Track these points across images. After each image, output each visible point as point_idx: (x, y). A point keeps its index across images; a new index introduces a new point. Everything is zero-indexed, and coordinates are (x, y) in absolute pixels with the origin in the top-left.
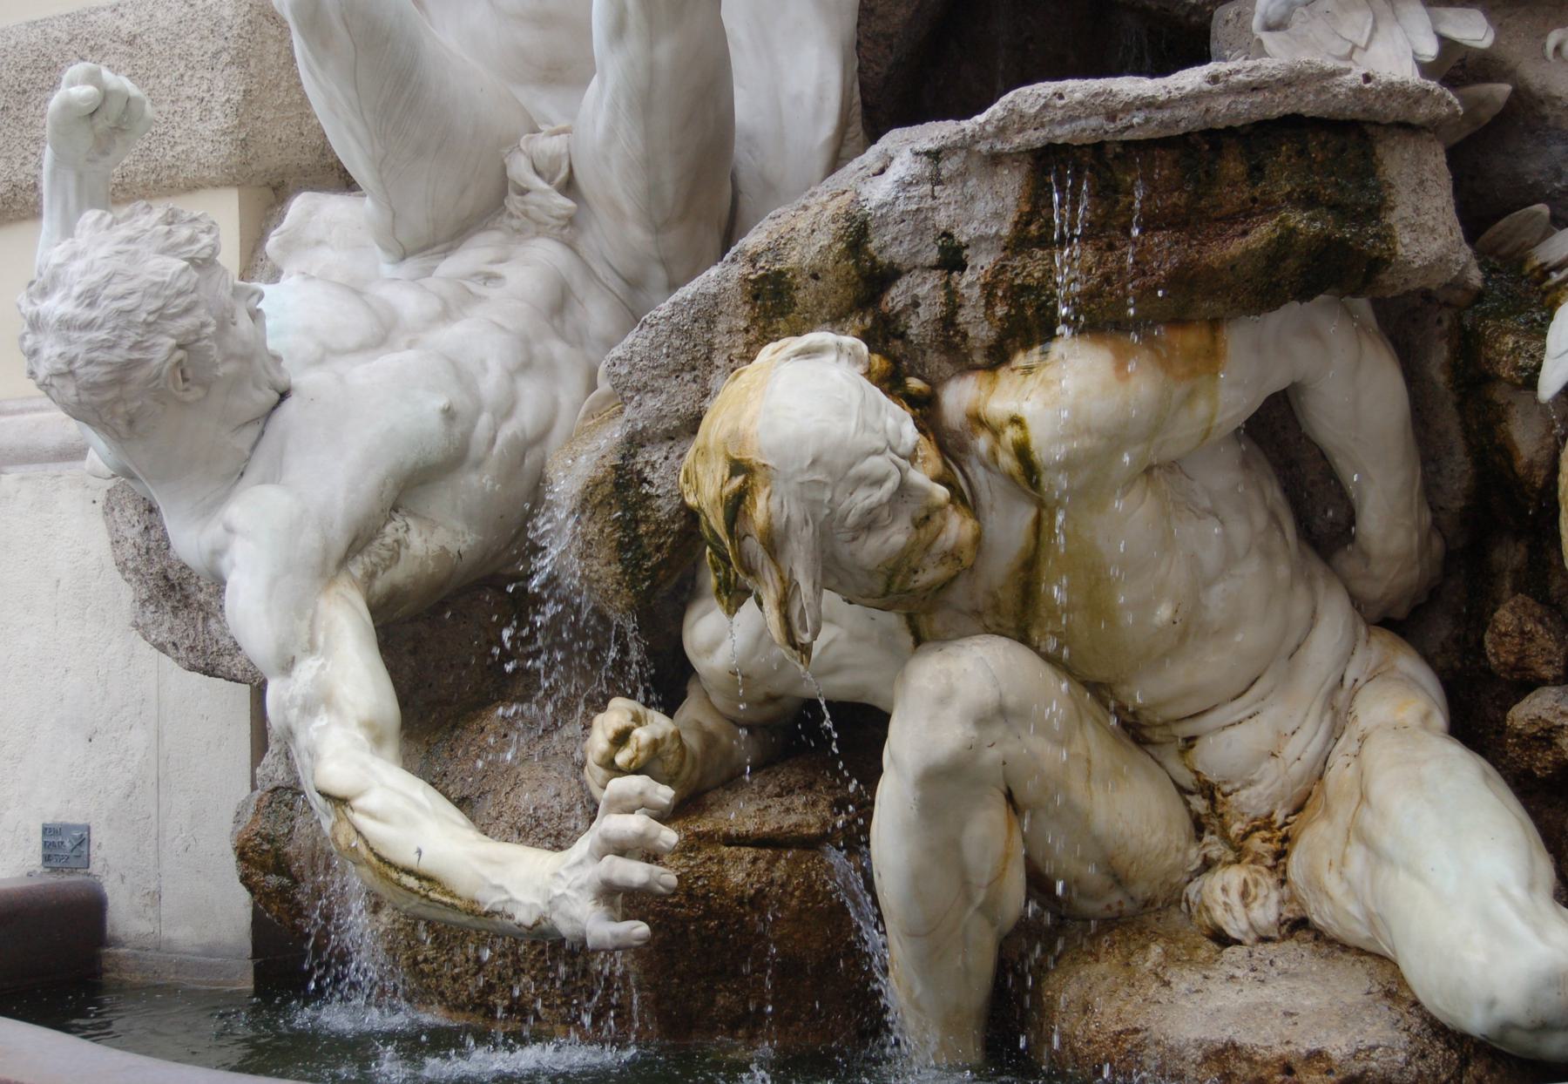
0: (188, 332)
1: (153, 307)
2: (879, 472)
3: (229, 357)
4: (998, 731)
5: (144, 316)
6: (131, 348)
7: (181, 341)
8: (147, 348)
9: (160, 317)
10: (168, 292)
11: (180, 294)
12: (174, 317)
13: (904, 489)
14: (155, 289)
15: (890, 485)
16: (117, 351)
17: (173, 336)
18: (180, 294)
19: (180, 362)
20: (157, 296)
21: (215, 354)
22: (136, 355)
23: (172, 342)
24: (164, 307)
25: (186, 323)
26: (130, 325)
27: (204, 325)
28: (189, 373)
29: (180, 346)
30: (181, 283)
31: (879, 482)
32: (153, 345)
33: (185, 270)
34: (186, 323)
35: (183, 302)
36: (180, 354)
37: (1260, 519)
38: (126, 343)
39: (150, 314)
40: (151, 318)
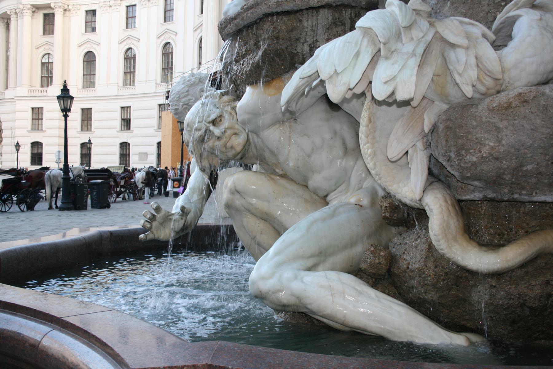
4: (238, 196)
6: (175, 105)
12: (182, 98)
15: (203, 130)
18: (183, 93)
22: (176, 107)
23: (181, 104)
25: (184, 100)
26: (174, 101)
27: (189, 100)
29: (186, 104)
30: (182, 91)
31: (199, 130)
35: (183, 95)
36: (185, 106)
37: (328, 136)
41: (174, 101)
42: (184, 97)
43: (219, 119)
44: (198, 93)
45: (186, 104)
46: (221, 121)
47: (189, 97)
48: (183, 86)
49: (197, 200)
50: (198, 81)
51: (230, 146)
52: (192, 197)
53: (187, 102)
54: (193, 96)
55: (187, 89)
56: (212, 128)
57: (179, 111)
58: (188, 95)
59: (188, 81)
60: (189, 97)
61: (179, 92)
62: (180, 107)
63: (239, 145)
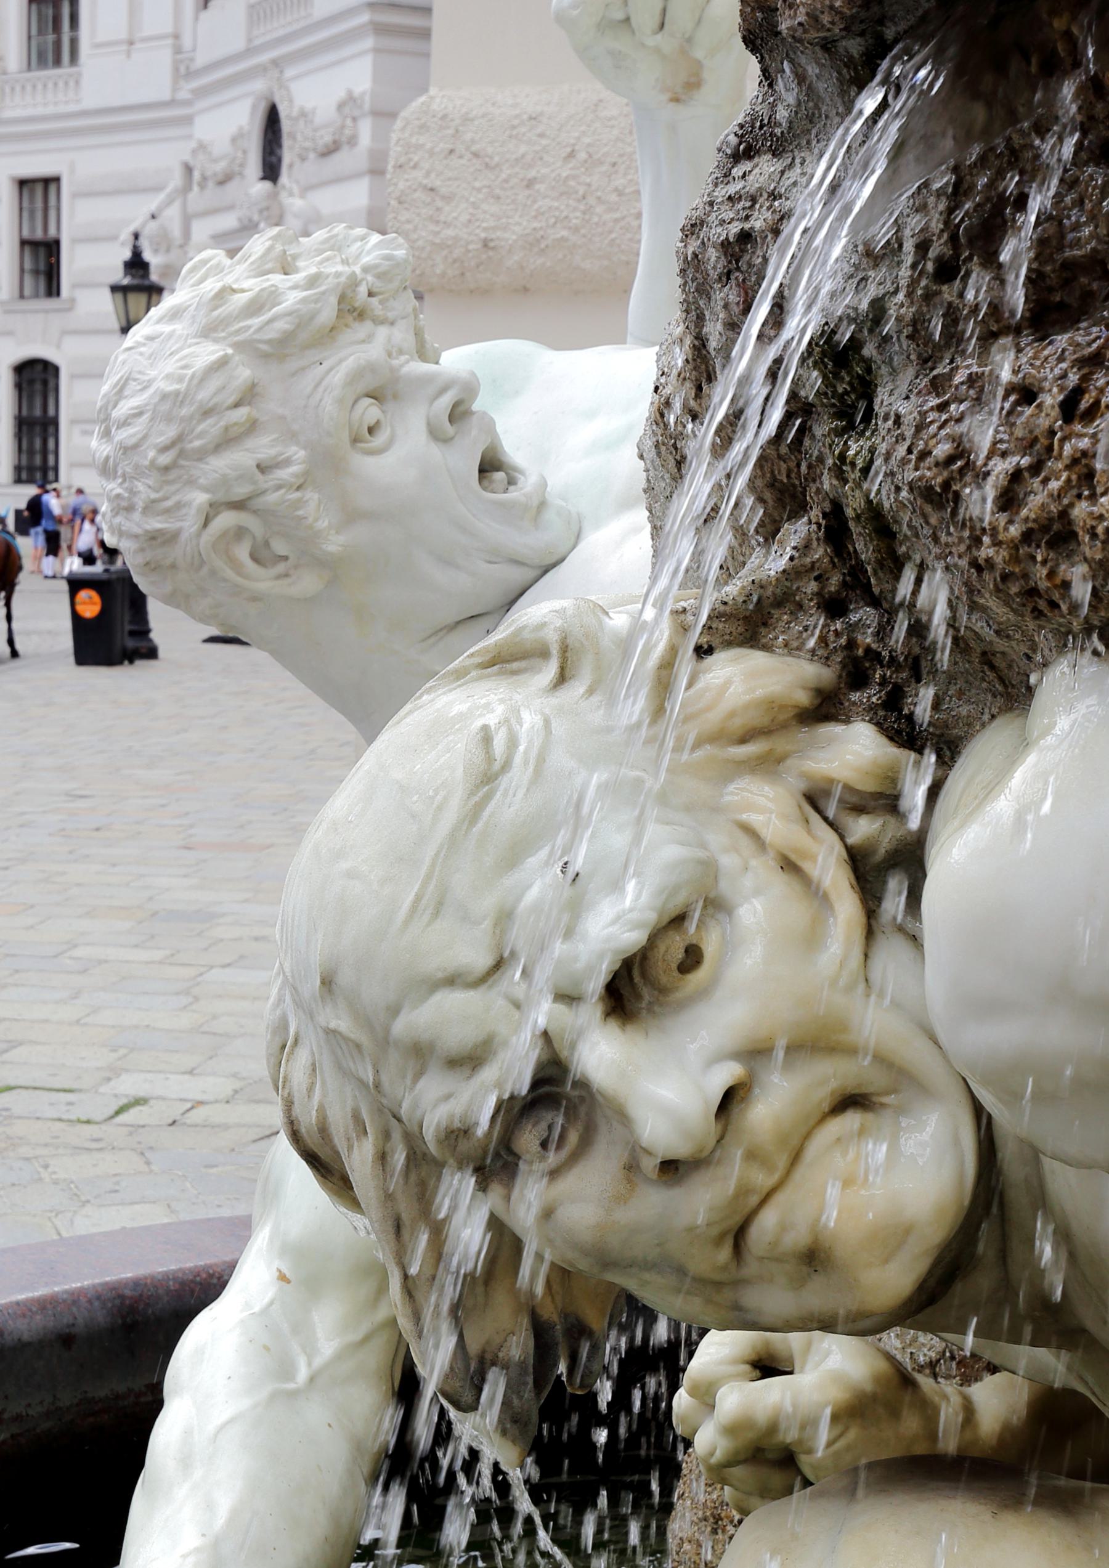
0: (225, 482)
1: (161, 440)
2: (459, 1037)
3: (351, 516)
5: (151, 454)
6: (149, 508)
7: (221, 496)
8: (167, 511)
9: (182, 454)
10: (184, 412)
11: (207, 412)
12: (201, 455)
13: (554, 1093)
14: (165, 407)
16: (137, 516)
17: (206, 490)
18: (207, 412)
19: (240, 533)
20: (169, 419)
21: (316, 510)
22: (156, 524)
23: (200, 498)
24: (179, 439)
25: (220, 464)
27: (262, 468)
28: (280, 547)
29: (239, 505)
30: (203, 395)
32: (179, 506)
33: (222, 363)
34: (240, 458)
35: (211, 428)
36: (226, 520)
38: (140, 505)
39: (165, 449)
40: (165, 459)
41: (140, 472)
42: (227, 440)
43: (674, 948)
44: (329, 406)
45: (239, 505)
46: (692, 958)
47: (263, 446)
48: (208, 353)
49: (339, 1357)
50: (328, 313)
51: (797, 1238)
52: (301, 1328)
53: (241, 491)
54: (292, 436)
55: (244, 373)
56: (602, 1054)
57: (178, 552)
58: (252, 427)
59: (255, 307)
60: (263, 446)
61: (177, 399)
62: (189, 524)
63: (892, 1237)
